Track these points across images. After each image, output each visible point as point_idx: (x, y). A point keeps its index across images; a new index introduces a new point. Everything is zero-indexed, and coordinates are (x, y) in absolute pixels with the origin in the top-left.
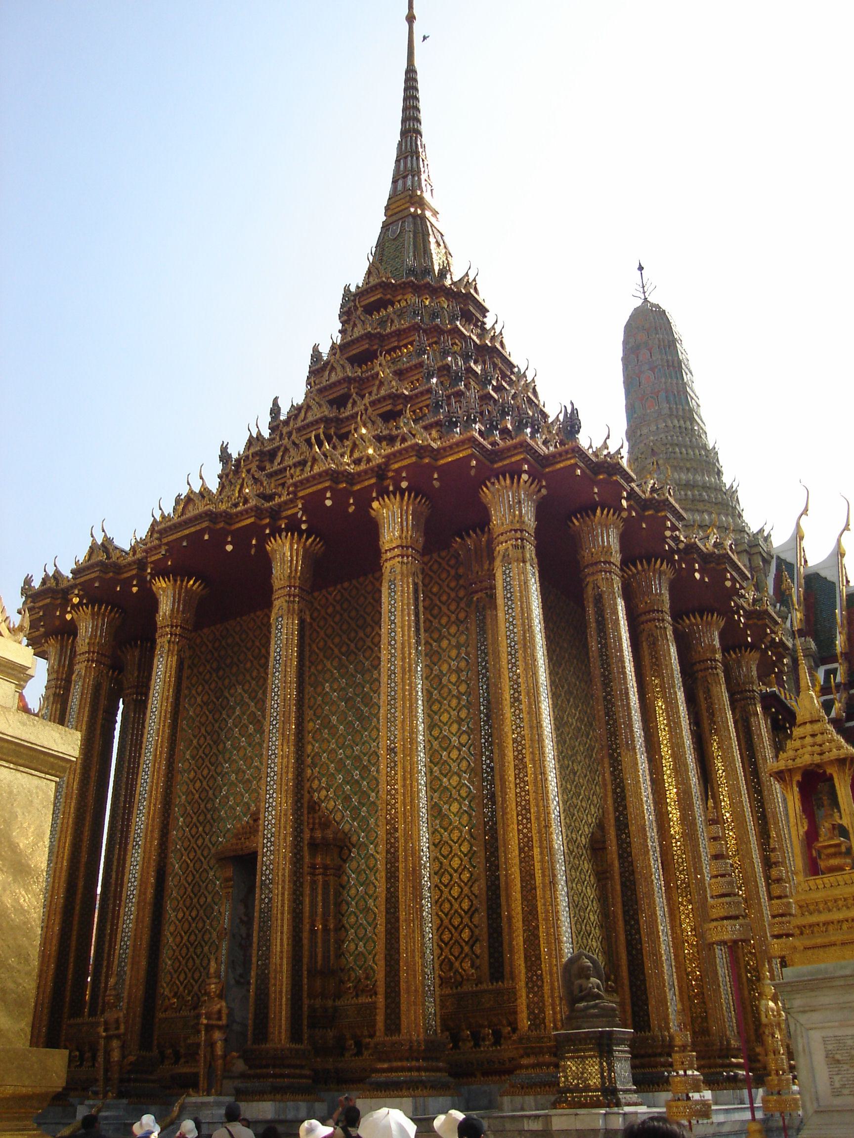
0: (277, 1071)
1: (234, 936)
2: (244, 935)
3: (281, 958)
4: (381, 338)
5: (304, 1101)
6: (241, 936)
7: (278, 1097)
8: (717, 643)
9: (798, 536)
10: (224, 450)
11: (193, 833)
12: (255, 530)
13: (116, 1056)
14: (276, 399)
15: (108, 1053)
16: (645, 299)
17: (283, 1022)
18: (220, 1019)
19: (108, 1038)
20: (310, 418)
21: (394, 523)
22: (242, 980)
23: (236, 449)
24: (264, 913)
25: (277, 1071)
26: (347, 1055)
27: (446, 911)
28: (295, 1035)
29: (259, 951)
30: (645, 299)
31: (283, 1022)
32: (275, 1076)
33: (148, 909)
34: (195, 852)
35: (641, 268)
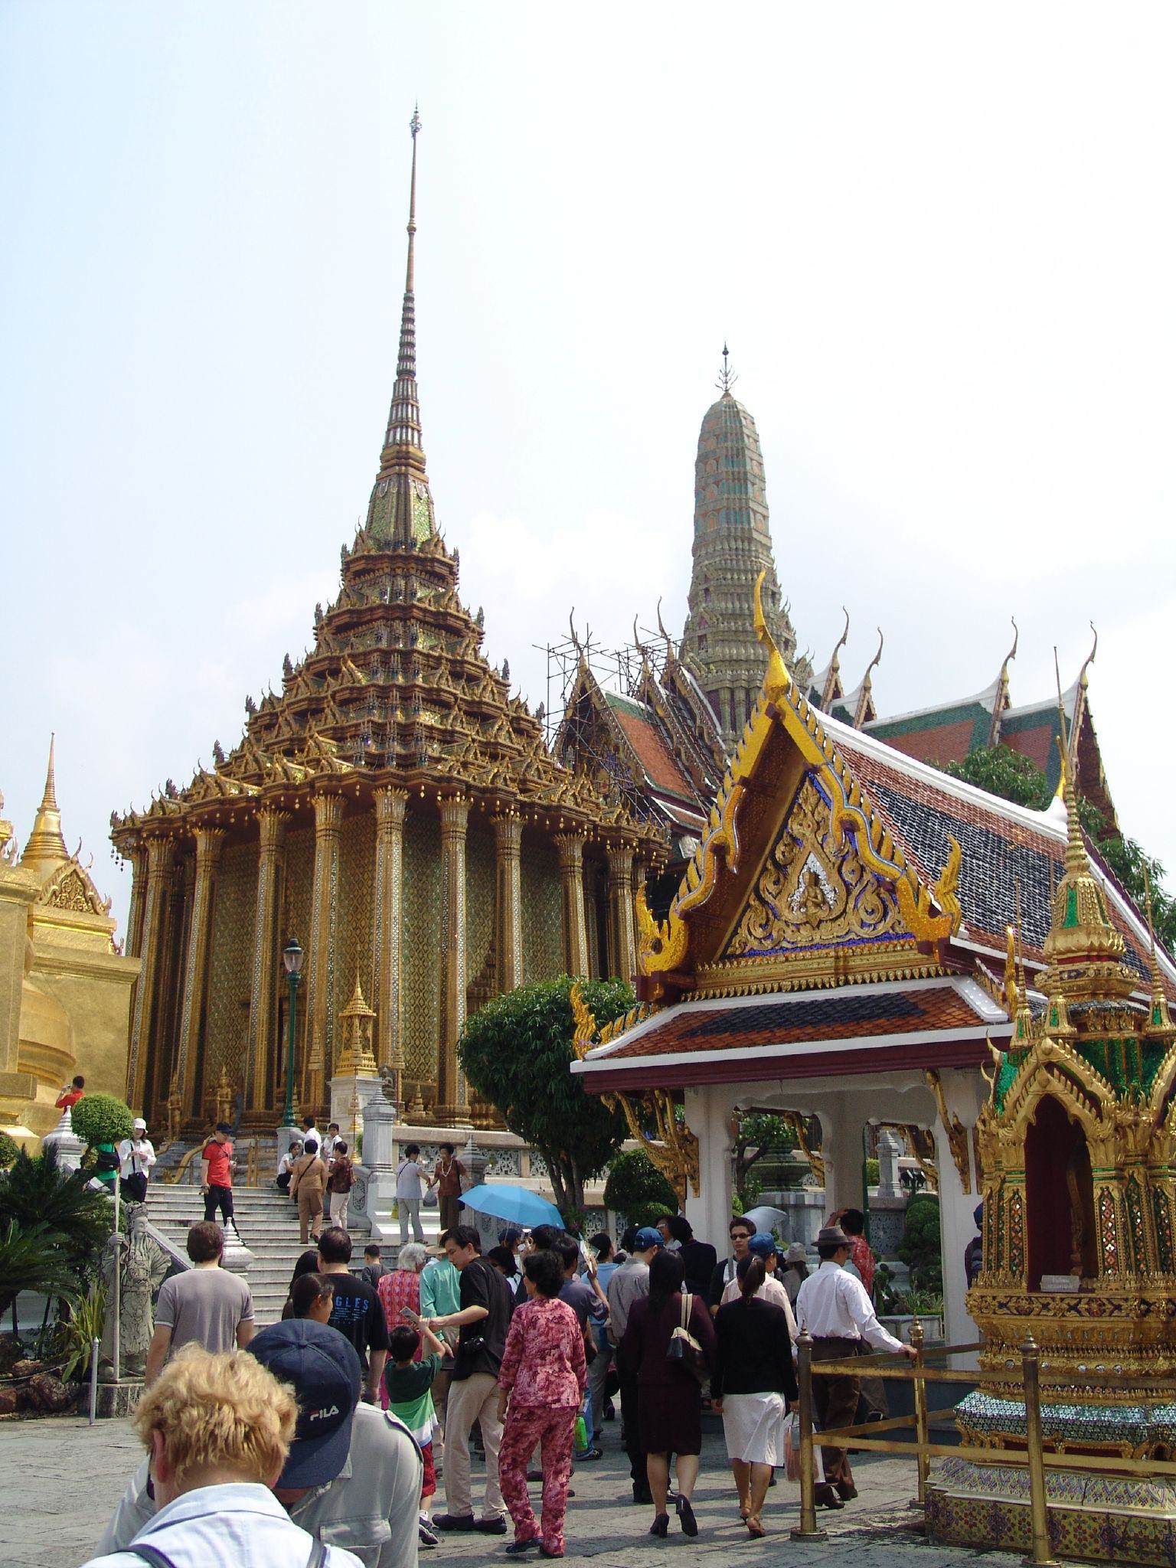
4: (360, 612)
8: (578, 853)
9: (834, 669)
10: (249, 702)
12: (247, 810)
13: (177, 1119)
14: (287, 657)
15: (173, 1117)
16: (727, 394)
19: (173, 1110)
20: (300, 697)
21: (324, 812)
23: (258, 707)
28: (268, 1105)
30: (727, 394)
33: (196, 1038)
35: (726, 353)
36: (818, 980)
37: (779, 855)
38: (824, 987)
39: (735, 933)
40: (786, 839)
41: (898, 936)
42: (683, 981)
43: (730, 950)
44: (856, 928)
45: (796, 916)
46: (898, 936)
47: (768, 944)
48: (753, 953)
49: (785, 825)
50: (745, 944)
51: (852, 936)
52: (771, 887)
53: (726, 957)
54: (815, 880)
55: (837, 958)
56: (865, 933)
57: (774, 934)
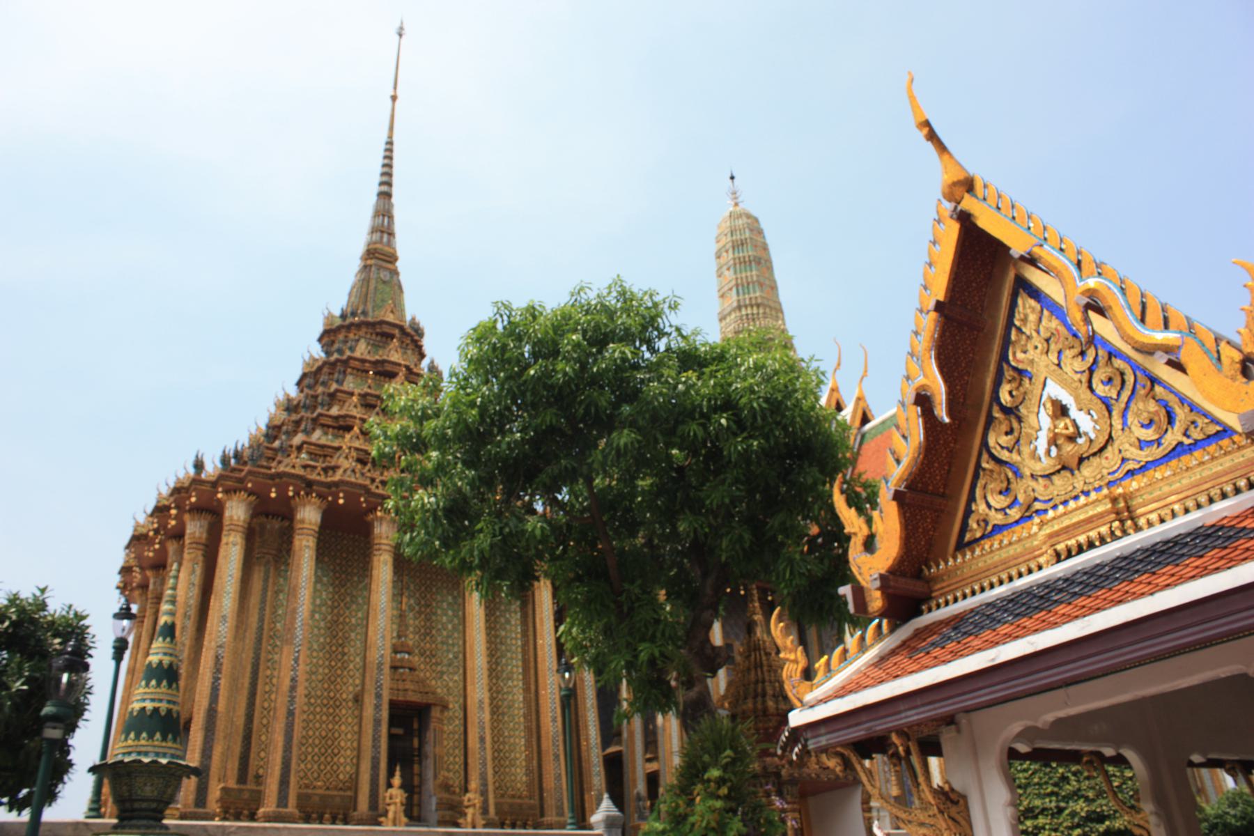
36: (1093, 534)
37: (1005, 398)
38: (1103, 541)
39: (968, 512)
40: (1008, 374)
41: (1196, 444)
42: (909, 586)
43: (968, 537)
44: (1132, 452)
45: (1046, 464)
46: (1196, 444)
47: (1015, 513)
48: (998, 529)
49: (1004, 357)
50: (986, 522)
51: (1131, 465)
52: (1004, 440)
53: (961, 546)
54: (1061, 411)
55: (1114, 500)
56: (1145, 456)
57: (1021, 498)
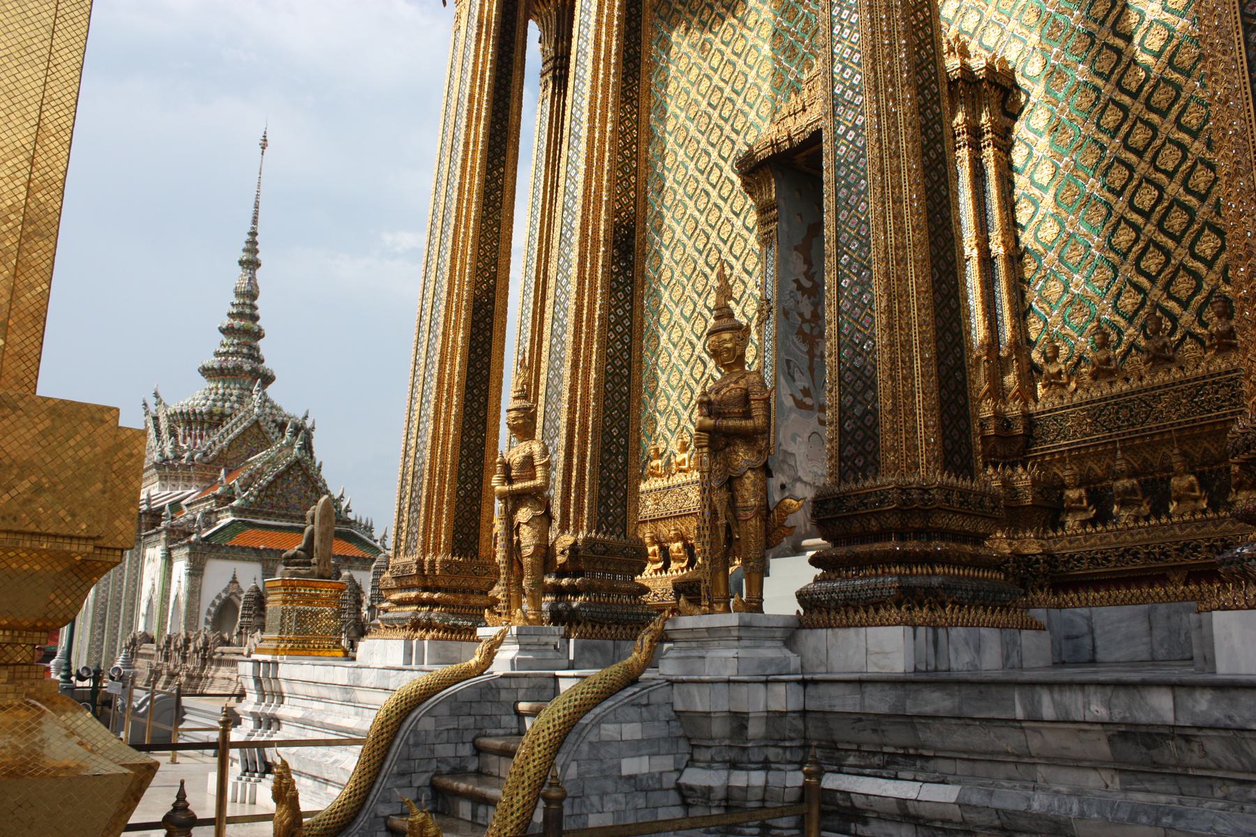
0: (912, 545)
1: (786, 313)
2: (808, 316)
3: (901, 261)
5: (992, 625)
6: (801, 315)
7: (922, 614)
11: (702, 165)
17: (920, 421)
18: (747, 415)
22: (808, 401)
24: (848, 164)
25: (912, 545)
26: (1071, 521)
27: (1183, 295)
29: (839, 256)
31: (920, 421)
32: (905, 559)
34: (707, 194)
